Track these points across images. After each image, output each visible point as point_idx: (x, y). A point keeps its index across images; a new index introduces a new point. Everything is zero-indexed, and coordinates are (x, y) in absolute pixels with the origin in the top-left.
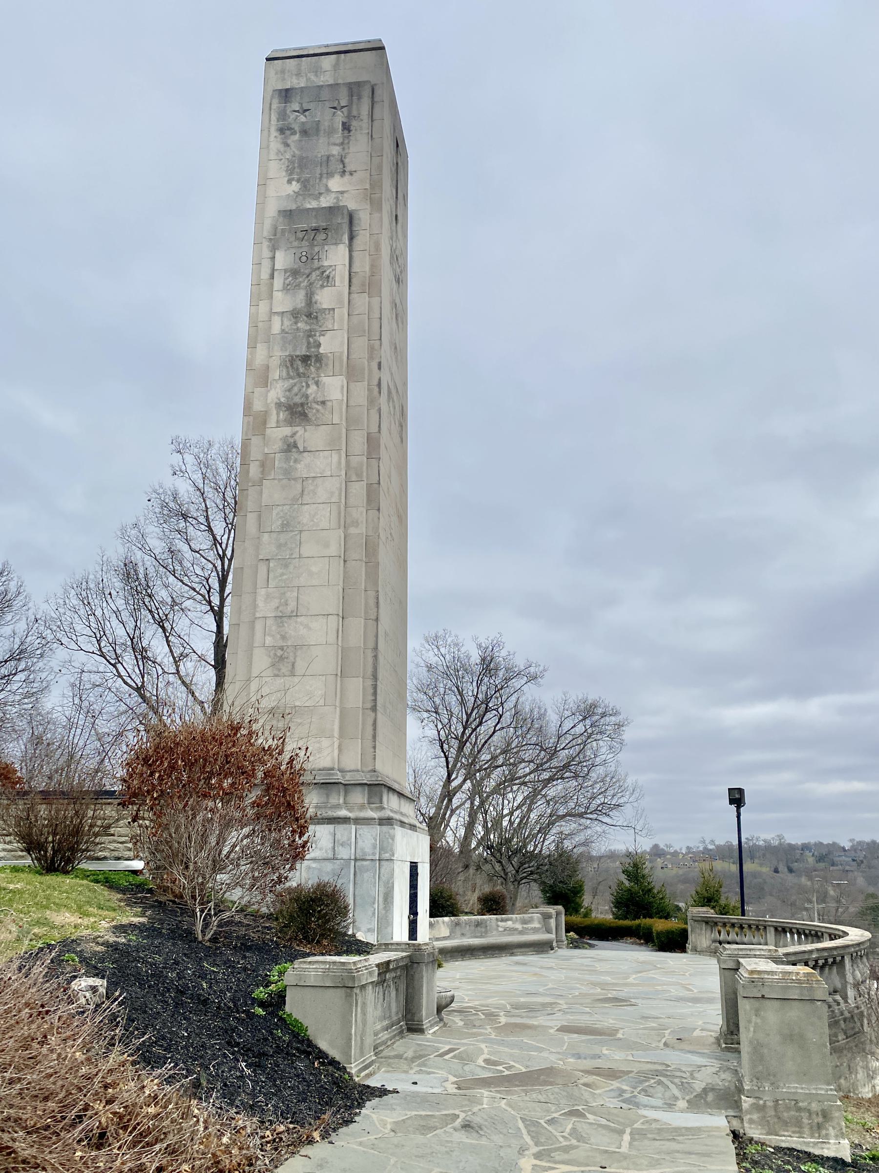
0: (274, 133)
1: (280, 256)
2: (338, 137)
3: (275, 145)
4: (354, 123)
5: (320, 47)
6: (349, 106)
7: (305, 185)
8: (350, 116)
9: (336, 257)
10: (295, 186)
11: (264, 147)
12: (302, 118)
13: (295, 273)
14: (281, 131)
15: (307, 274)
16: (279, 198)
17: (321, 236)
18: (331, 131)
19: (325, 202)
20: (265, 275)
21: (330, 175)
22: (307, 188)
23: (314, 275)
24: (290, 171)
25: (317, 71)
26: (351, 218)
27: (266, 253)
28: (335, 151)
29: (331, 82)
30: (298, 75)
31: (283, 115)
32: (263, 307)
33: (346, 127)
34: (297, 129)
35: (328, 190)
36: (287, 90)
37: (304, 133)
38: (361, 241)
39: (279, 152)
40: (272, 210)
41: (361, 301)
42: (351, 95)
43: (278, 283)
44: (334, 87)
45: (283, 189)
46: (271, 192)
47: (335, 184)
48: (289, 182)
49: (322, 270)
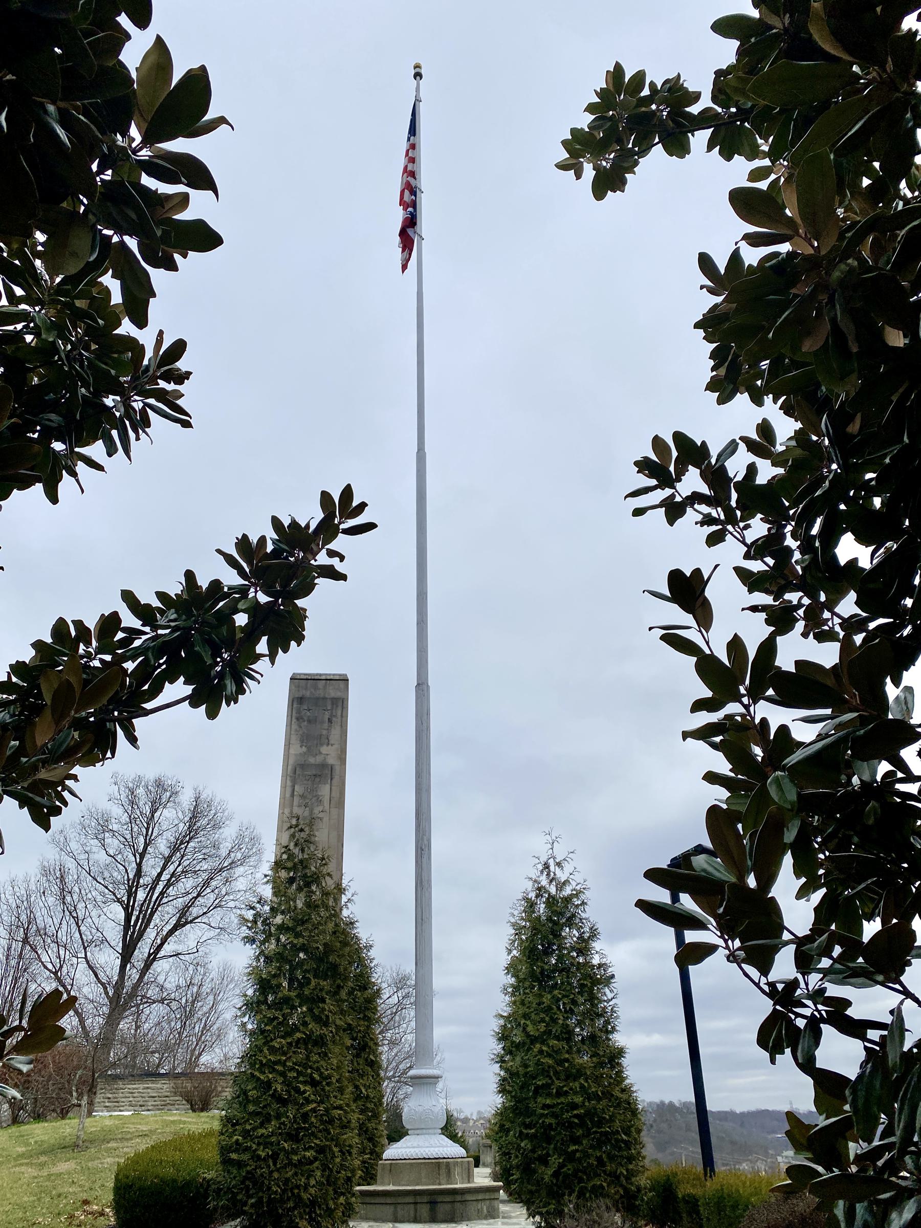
0: (294, 720)
1: (297, 788)
2: (326, 725)
3: (294, 727)
4: (334, 719)
5: (317, 675)
6: (332, 709)
7: (309, 748)
8: (332, 715)
9: (325, 791)
10: (304, 749)
11: (289, 725)
12: (308, 714)
13: (302, 796)
14: (297, 719)
15: (309, 798)
16: (296, 755)
17: (318, 779)
18: (322, 722)
19: (319, 759)
20: (288, 795)
21: (322, 745)
22: (310, 751)
23: (313, 800)
24: (302, 741)
25: (316, 688)
26: (332, 767)
27: (289, 783)
28: (324, 732)
29: (322, 696)
30: (306, 689)
31: (299, 712)
32: (287, 811)
33: (330, 721)
34: (306, 718)
35: (320, 753)
36: (301, 698)
37: (309, 721)
38: (335, 781)
39: (296, 730)
40: (291, 762)
41: (334, 811)
42: (333, 704)
43: (296, 799)
44: (325, 698)
45: (296, 749)
46: (292, 751)
47: (324, 749)
48: (301, 746)
49: (317, 797)
